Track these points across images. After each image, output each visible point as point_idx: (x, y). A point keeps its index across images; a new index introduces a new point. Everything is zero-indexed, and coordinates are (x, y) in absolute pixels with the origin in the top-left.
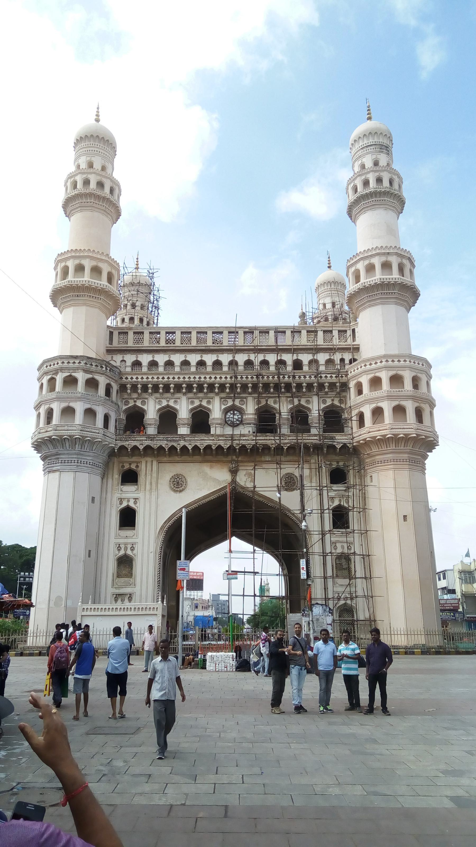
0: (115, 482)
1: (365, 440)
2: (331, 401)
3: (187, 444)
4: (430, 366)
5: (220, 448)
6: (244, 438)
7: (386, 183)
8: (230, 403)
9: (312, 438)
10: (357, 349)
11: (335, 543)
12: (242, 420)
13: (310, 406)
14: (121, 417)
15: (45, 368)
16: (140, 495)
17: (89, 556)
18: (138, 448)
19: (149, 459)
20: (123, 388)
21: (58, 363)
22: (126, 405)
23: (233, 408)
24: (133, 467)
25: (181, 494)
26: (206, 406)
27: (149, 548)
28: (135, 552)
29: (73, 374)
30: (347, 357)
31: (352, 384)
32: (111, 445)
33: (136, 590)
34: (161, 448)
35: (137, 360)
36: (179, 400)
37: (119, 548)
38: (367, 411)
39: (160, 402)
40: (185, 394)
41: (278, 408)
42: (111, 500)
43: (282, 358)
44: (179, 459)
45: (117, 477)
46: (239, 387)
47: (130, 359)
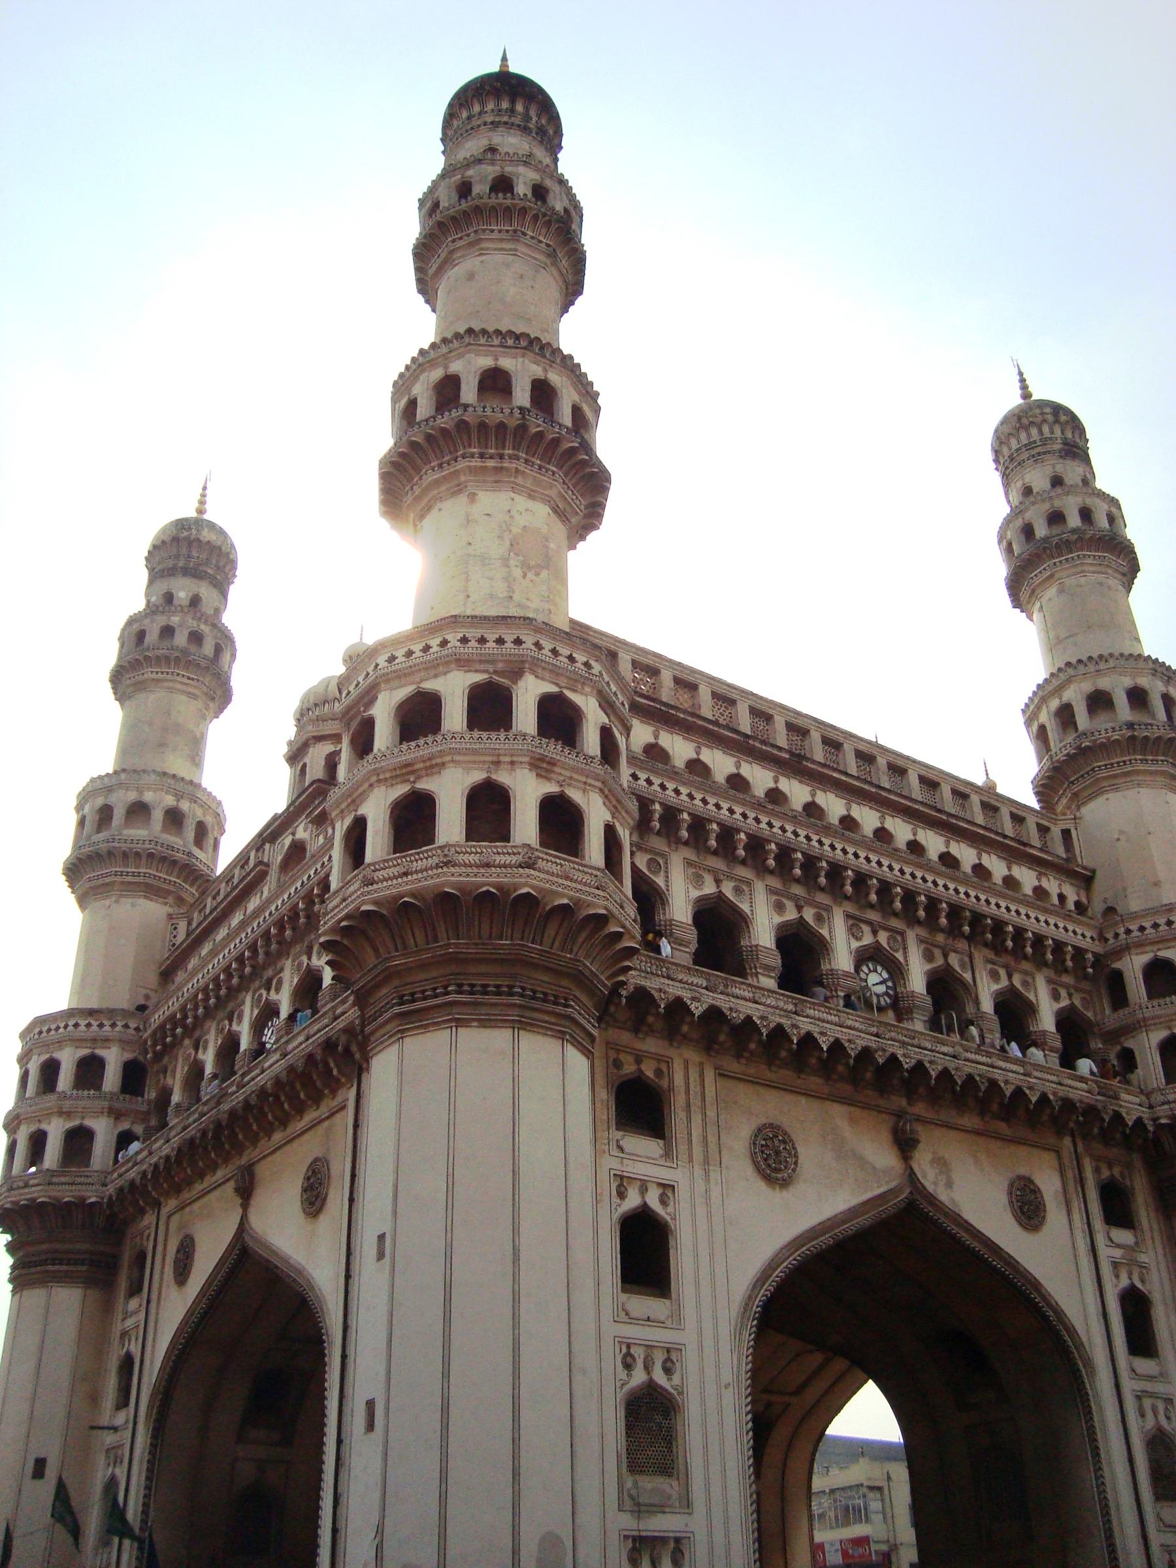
0: (603, 1115)
3: (815, 1030)
6: (945, 1049)
10: (1086, 880)
12: (896, 993)
24: (649, 1071)
25: (785, 1193)
26: (812, 924)
27: (718, 1365)
28: (676, 1379)
29: (568, 693)
37: (629, 1359)
39: (698, 881)
41: (971, 981)
44: (769, 1075)
46: (898, 894)
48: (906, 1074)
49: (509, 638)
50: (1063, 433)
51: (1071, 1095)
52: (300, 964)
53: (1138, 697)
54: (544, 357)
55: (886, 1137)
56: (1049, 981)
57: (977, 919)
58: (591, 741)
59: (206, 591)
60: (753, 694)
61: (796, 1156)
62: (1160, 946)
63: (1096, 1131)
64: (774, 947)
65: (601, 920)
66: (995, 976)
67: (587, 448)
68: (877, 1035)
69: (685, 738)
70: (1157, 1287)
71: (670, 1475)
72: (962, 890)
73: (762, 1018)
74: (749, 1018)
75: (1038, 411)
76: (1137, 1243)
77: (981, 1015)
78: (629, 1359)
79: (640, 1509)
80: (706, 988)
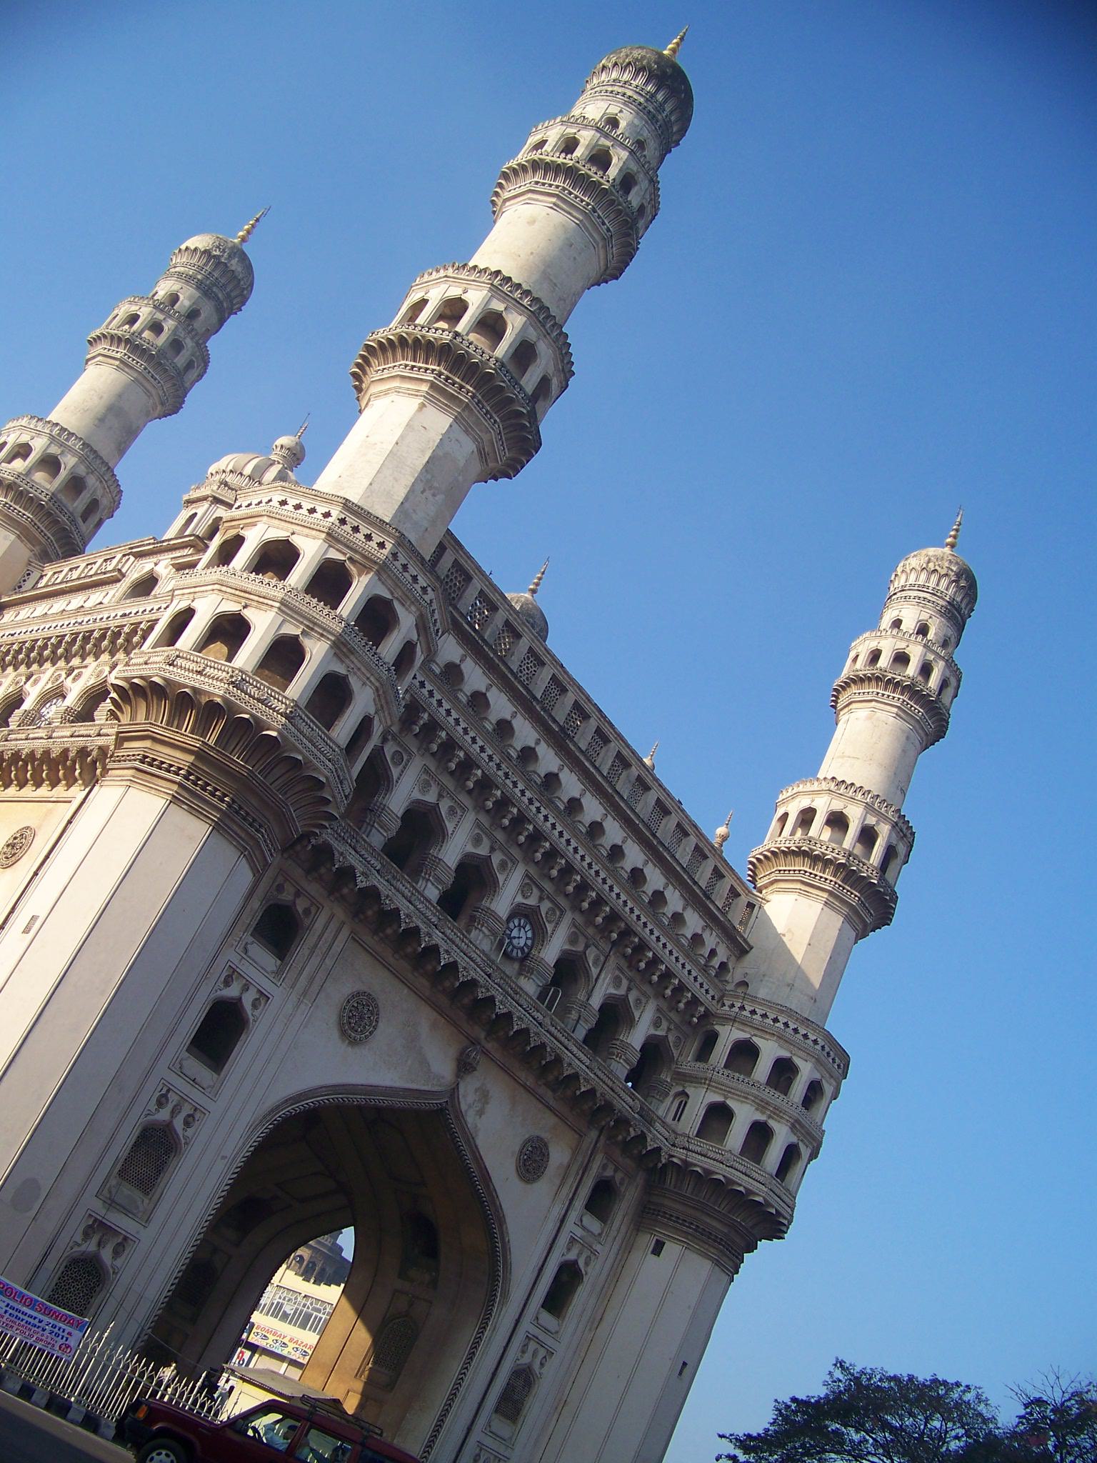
0: (246, 918)
3: (443, 946)
6: (536, 1014)
10: (741, 949)
18: (355, 877)
19: (340, 914)
24: (301, 906)
28: (190, 1132)
29: (396, 604)
33: (146, 1236)
37: (163, 1100)
39: (425, 787)
40: (480, 807)
44: (391, 960)
49: (377, 539)
51: (615, 1102)
52: (101, 672)
53: (867, 836)
54: (544, 326)
55: (453, 1052)
56: (659, 1010)
57: (628, 932)
58: (390, 647)
59: (207, 310)
61: (375, 1028)
62: (759, 1033)
63: (620, 1137)
64: (453, 867)
65: (320, 785)
66: (617, 982)
67: (534, 418)
68: (489, 976)
70: (593, 1274)
72: (630, 904)
73: (408, 916)
74: (397, 910)
75: (946, 564)
76: (600, 1235)
77: (585, 1005)
78: (163, 1100)
79: (111, 1203)
80: (378, 871)
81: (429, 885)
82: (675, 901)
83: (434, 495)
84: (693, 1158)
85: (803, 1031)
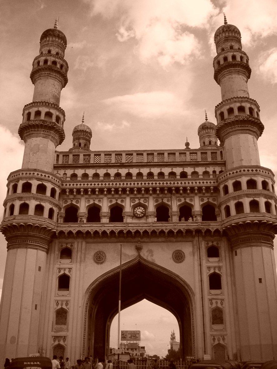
1: (231, 225)
2: (207, 199)
4: (274, 175)
5: (129, 232)
6: (147, 225)
7: (238, 59)
8: (137, 201)
9: (194, 225)
10: (224, 164)
11: (211, 300)
13: (193, 203)
14: (62, 212)
15: (11, 178)
16: (73, 266)
17: (36, 309)
19: (80, 240)
20: (63, 192)
21: (19, 174)
22: (65, 203)
23: (140, 205)
25: (102, 265)
27: (78, 303)
28: (68, 307)
29: (29, 181)
30: (218, 169)
31: (222, 187)
32: (54, 230)
33: (69, 334)
34: (88, 233)
35: (74, 173)
36: (101, 200)
37: (58, 304)
38: (232, 205)
40: (106, 195)
42: (53, 268)
43: (173, 171)
45: (57, 252)
47: (70, 172)
48: (133, 234)
50: (225, 34)
51: (190, 228)
55: (133, 247)
56: (200, 197)
60: (115, 151)
62: (225, 182)
66: (180, 200)
68: (125, 227)
69: (93, 169)
71: (65, 325)
80: (78, 227)
81: (103, 219)
82: (189, 170)
83: (36, 154)
84: (226, 225)
85: (235, 172)
